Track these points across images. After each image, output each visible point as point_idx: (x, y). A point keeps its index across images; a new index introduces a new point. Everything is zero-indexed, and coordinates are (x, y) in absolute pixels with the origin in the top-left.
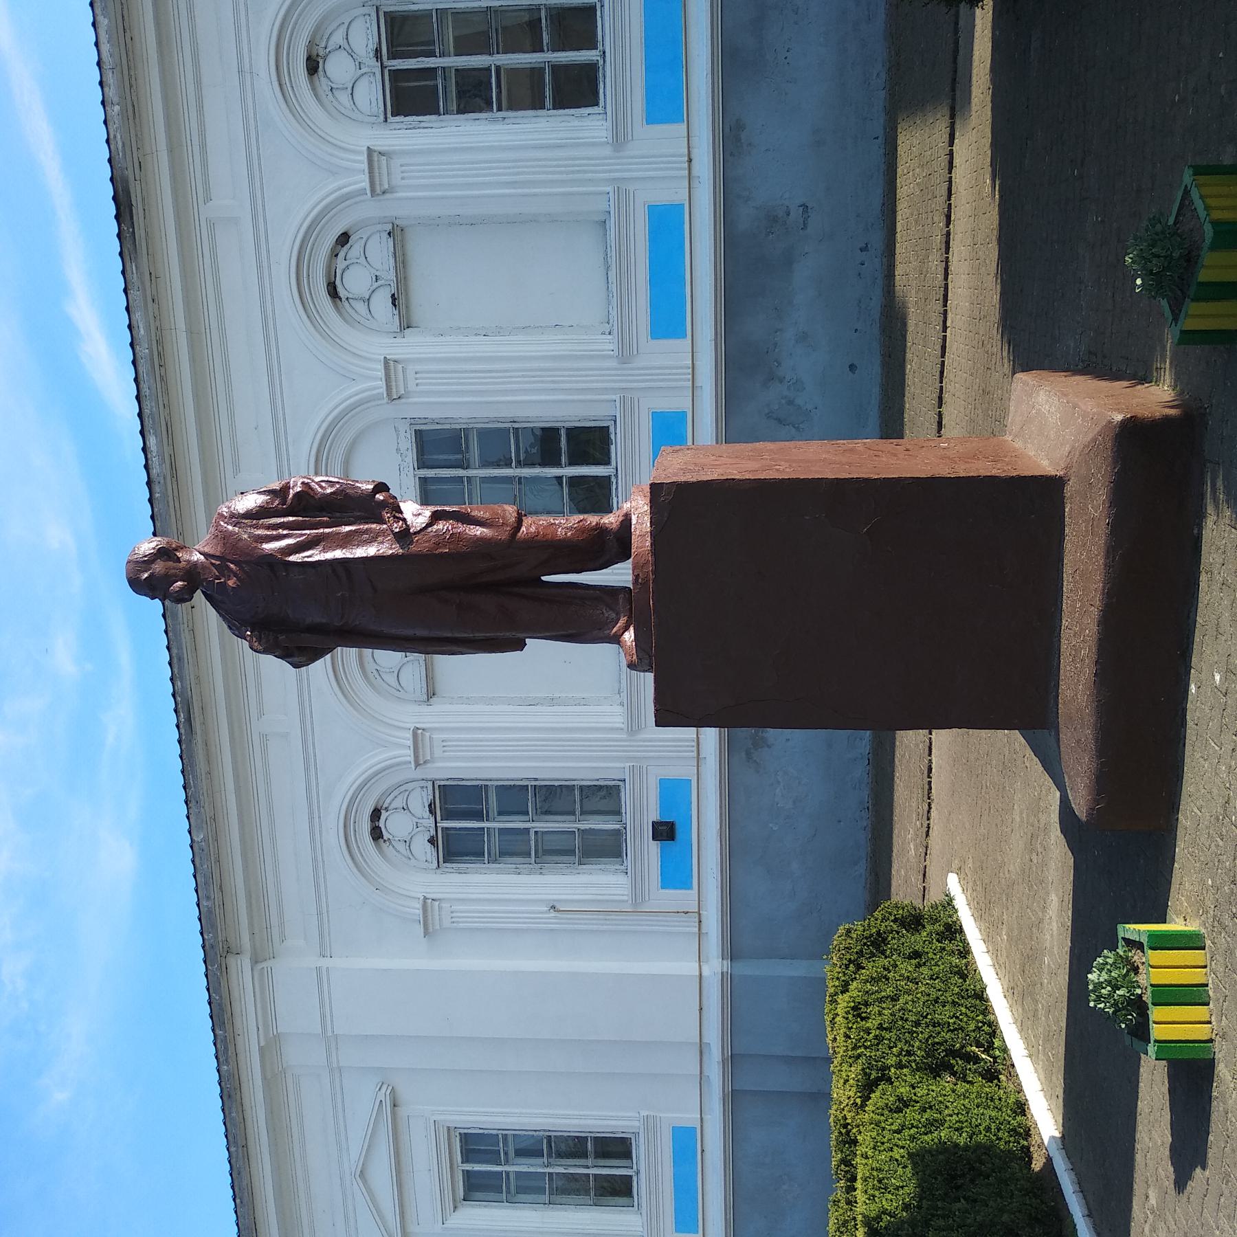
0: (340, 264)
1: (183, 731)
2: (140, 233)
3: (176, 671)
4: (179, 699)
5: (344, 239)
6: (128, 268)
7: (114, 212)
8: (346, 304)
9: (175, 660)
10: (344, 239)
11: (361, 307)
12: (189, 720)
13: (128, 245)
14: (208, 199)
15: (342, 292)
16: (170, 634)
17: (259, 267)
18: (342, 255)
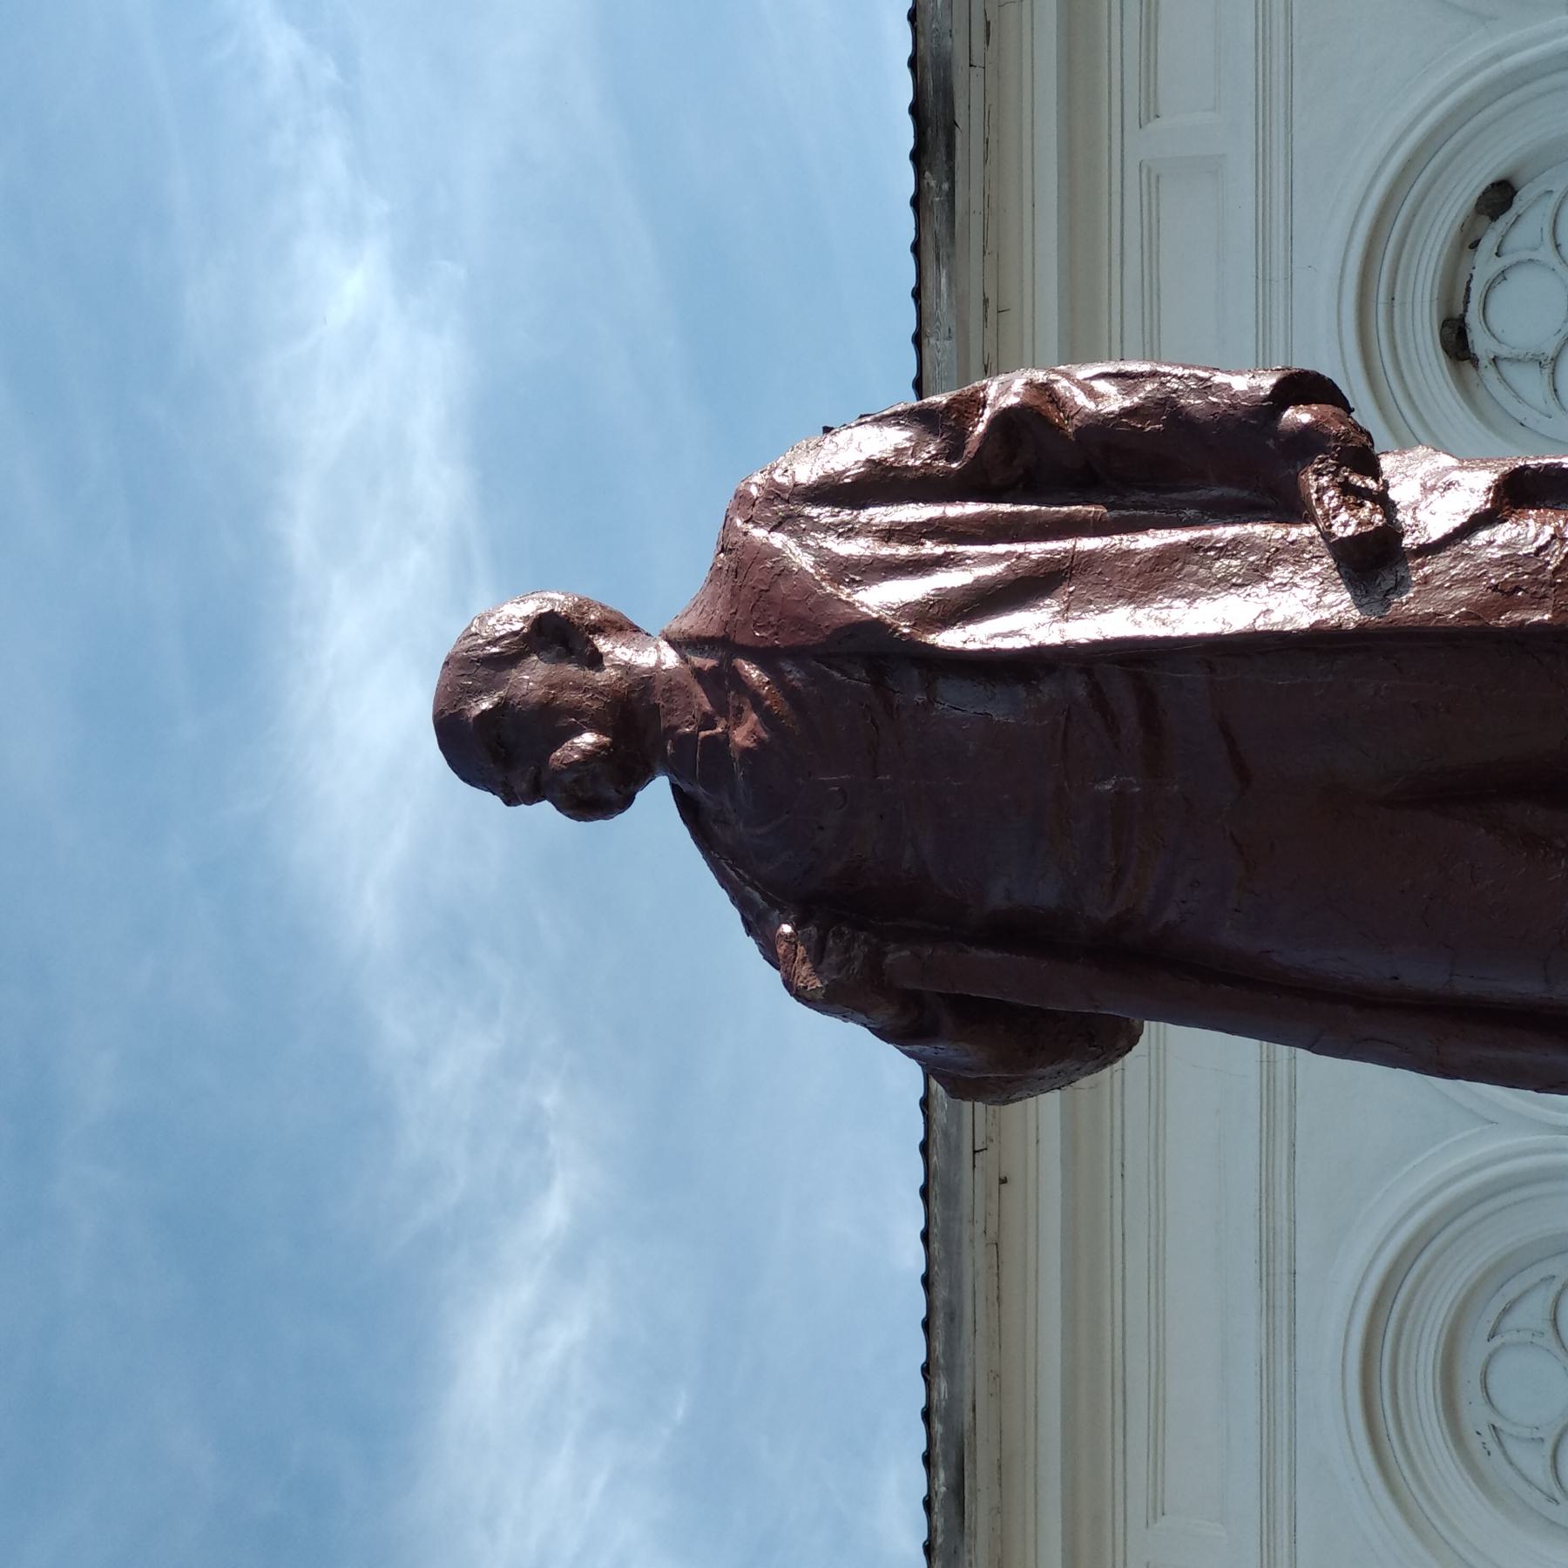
0: (1484, 265)
1: (939, 1522)
2: (969, 195)
3: (939, 1347)
4: (938, 1428)
5: (1499, 198)
6: (929, 283)
7: (910, 143)
8: (1490, 374)
9: (939, 1321)
10: (1499, 198)
11: (1531, 382)
12: (958, 1490)
13: (936, 224)
14: (1150, 112)
15: (1480, 343)
16: (935, 1245)
17: (1263, 279)
18: (1488, 244)
